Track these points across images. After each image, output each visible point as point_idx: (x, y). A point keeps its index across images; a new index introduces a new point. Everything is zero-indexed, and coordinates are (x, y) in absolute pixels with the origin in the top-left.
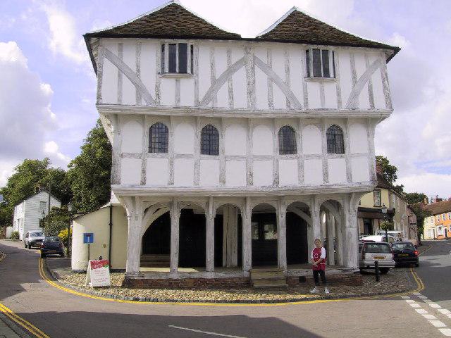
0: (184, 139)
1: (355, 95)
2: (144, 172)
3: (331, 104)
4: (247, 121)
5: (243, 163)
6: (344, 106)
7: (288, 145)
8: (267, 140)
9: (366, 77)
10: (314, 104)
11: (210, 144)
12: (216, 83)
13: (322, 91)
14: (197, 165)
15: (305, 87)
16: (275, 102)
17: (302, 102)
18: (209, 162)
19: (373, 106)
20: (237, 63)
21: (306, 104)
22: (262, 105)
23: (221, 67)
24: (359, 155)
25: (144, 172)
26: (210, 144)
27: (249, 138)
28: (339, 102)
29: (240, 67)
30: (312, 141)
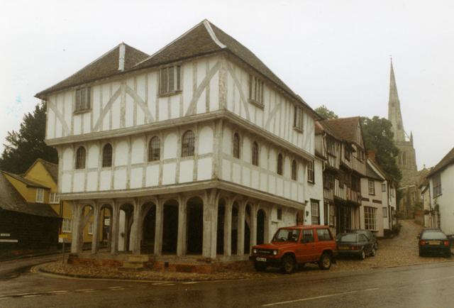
0: (94, 156)
1: (194, 103)
2: (72, 183)
3: (176, 115)
4: (130, 138)
5: (124, 171)
6: (184, 115)
7: (154, 155)
8: (140, 150)
9: (206, 84)
10: (163, 117)
11: (107, 161)
12: (103, 113)
13: (169, 103)
14: (178, 165)
15: (157, 102)
16: (137, 119)
17: (154, 114)
18: (107, 173)
19: (208, 109)
20: (115, 95)
21: (157, 118)
22: (129, 124)
23: (106, 100)
24: (206, 156)
25: (72, 183)
26: (107, 161)
27: (130, 150)
28: (181, 110)
29: (117, 97)
30: (171, 147)
